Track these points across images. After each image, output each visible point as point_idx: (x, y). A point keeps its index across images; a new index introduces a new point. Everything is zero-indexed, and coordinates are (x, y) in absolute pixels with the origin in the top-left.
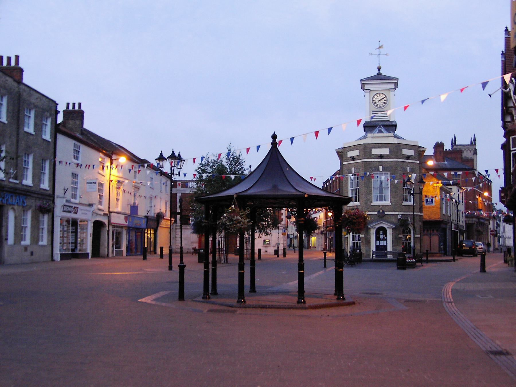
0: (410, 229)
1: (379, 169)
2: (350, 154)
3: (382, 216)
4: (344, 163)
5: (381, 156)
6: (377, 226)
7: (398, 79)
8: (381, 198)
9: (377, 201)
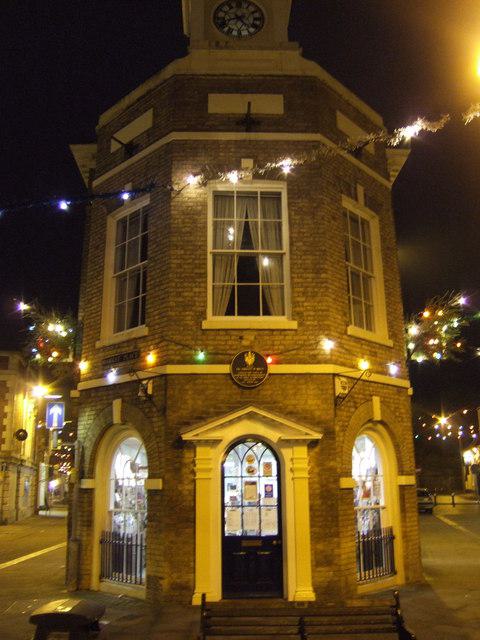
9: (230, 312)
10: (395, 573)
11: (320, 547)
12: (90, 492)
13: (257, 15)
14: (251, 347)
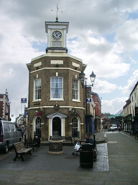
0: (77, 119)
1: (56, 75)
2: (36, 65)
3: (57, 109)
4: (31, 72)
5: (57, 66)
6: (54, 117)
7: (69, 22)
8: (57, 95)
10: (79, 138)
11: (66, 133)
12: (32, 125)
13: (60, 34)
14: (57, 103)
